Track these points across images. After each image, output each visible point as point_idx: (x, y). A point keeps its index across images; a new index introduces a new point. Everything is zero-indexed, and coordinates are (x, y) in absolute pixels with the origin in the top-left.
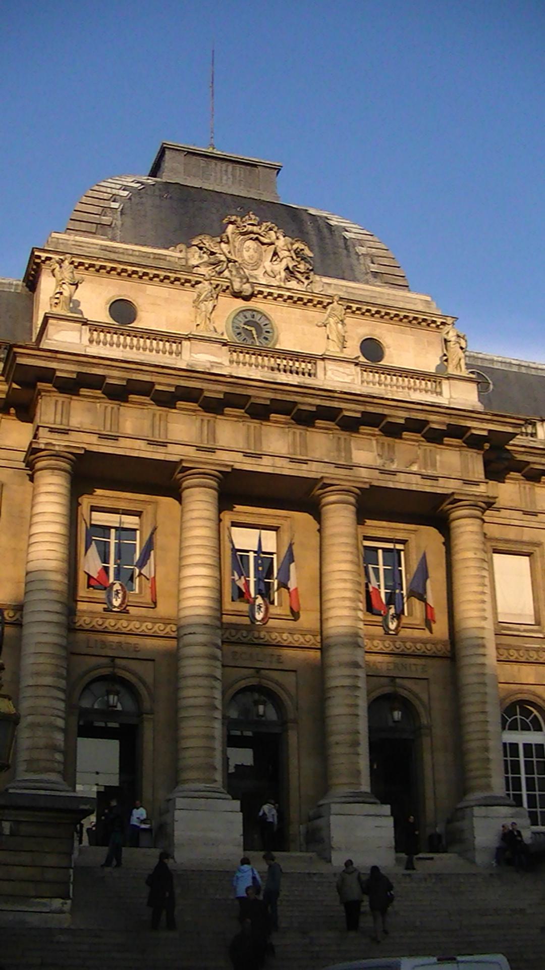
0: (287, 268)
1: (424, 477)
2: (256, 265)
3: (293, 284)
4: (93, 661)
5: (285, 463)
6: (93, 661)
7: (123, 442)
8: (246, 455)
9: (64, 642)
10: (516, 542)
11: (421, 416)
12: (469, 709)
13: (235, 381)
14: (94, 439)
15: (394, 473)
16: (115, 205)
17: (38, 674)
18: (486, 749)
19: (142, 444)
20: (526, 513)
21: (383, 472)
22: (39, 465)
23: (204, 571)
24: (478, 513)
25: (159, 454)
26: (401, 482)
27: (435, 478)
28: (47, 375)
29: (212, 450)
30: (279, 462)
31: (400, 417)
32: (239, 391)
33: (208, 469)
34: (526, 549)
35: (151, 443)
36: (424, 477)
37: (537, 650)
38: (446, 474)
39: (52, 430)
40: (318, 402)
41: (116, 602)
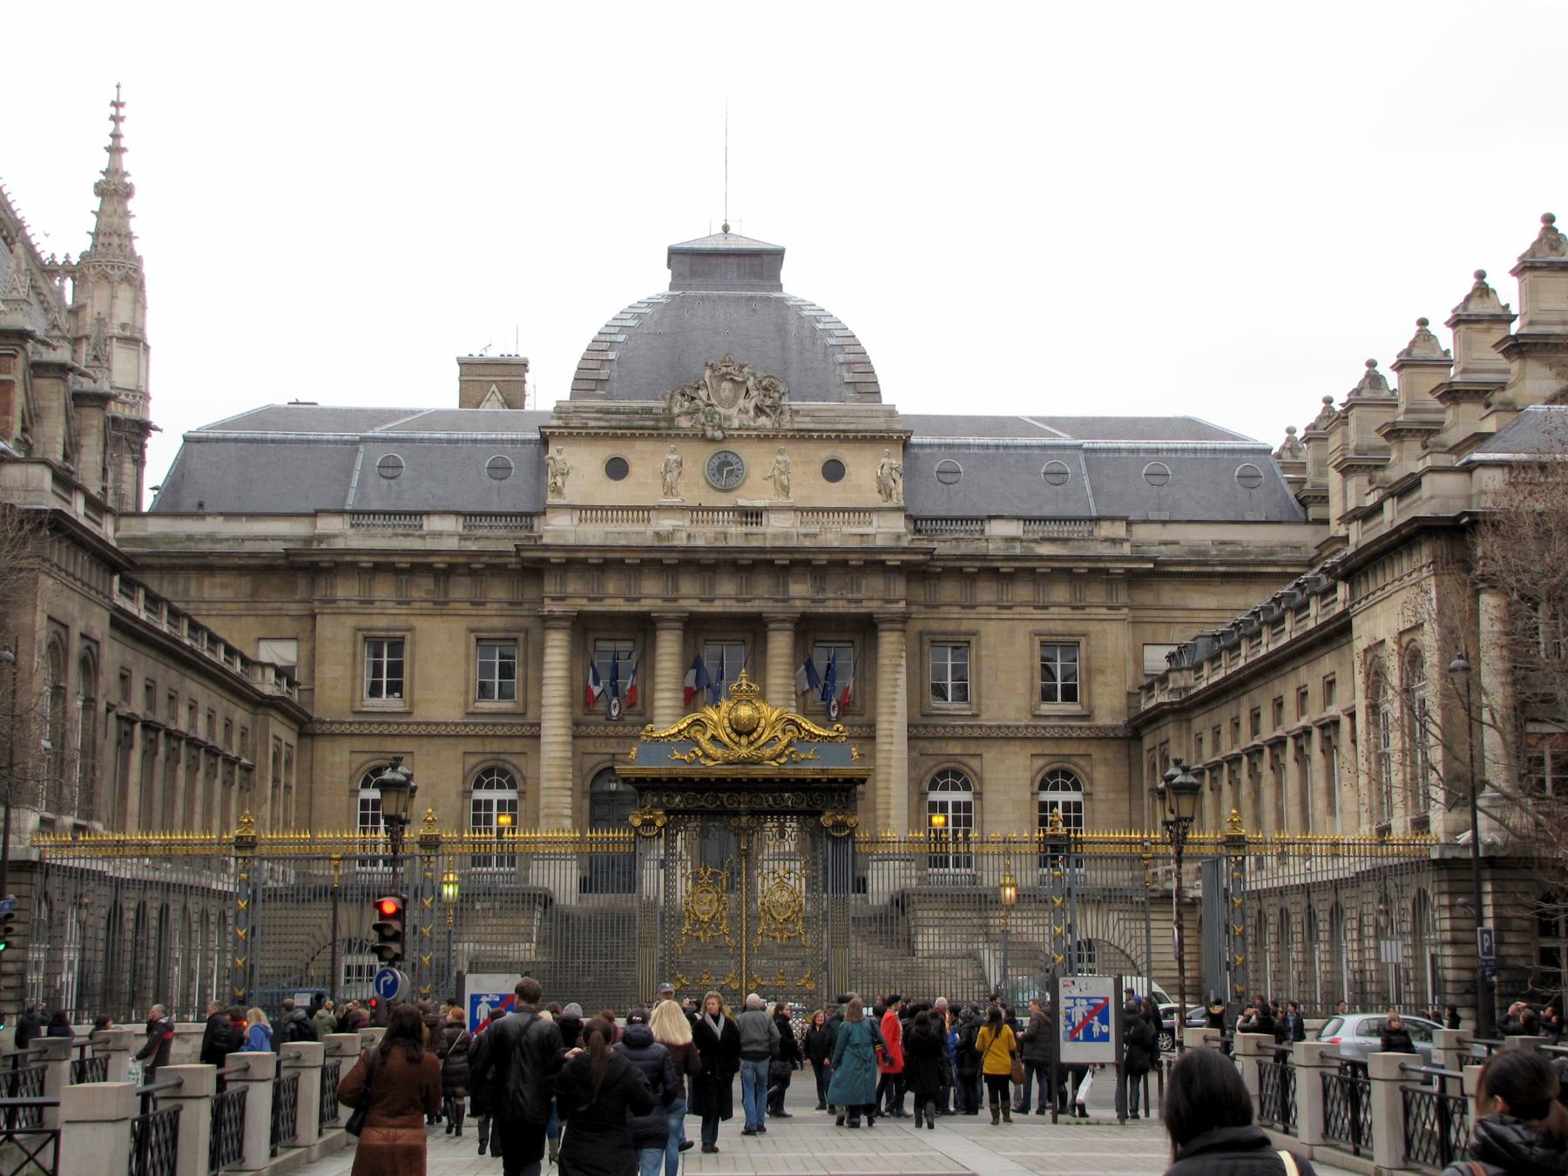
0: (757, 407)
1: (849, 601)
2: (732, 403)
3: (763, 420)
4: (597, 758)
5: (733, 603)
6: (597, 758)
7: (607, 602)
8: (702, 600)
9: (569, 755)
10: (952, 634)
11: (841, 557)
12: (879, 785)
13: (686, 550)
14: (585, 601)
15: (824, 601)
16: (612, 355)
17: (549, 780)
18: (888, 817)
19: (621, 601)
20: (964, 607)
21: (813, 601)
22: (549, 624)
23: (668, 695)
24: (899, 626)
25: (634, 608)
26: (829, 608)
27: (859, 601)
28: (546, 561)
29: (675, 600)
30: (728, 603)
31: (823, 559)
32: (690, 556)
33: (671, 615)
34: (962, 638)
35: (628, 599)
36: (849, 601)
37: (962, 727)
38: (869, 595)
39: (553, 599)
40: (753, 556)
41: (615, 713)
